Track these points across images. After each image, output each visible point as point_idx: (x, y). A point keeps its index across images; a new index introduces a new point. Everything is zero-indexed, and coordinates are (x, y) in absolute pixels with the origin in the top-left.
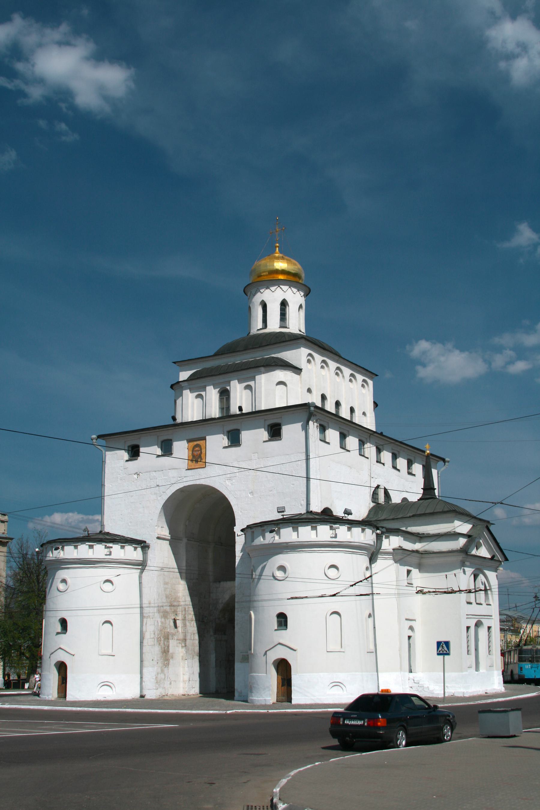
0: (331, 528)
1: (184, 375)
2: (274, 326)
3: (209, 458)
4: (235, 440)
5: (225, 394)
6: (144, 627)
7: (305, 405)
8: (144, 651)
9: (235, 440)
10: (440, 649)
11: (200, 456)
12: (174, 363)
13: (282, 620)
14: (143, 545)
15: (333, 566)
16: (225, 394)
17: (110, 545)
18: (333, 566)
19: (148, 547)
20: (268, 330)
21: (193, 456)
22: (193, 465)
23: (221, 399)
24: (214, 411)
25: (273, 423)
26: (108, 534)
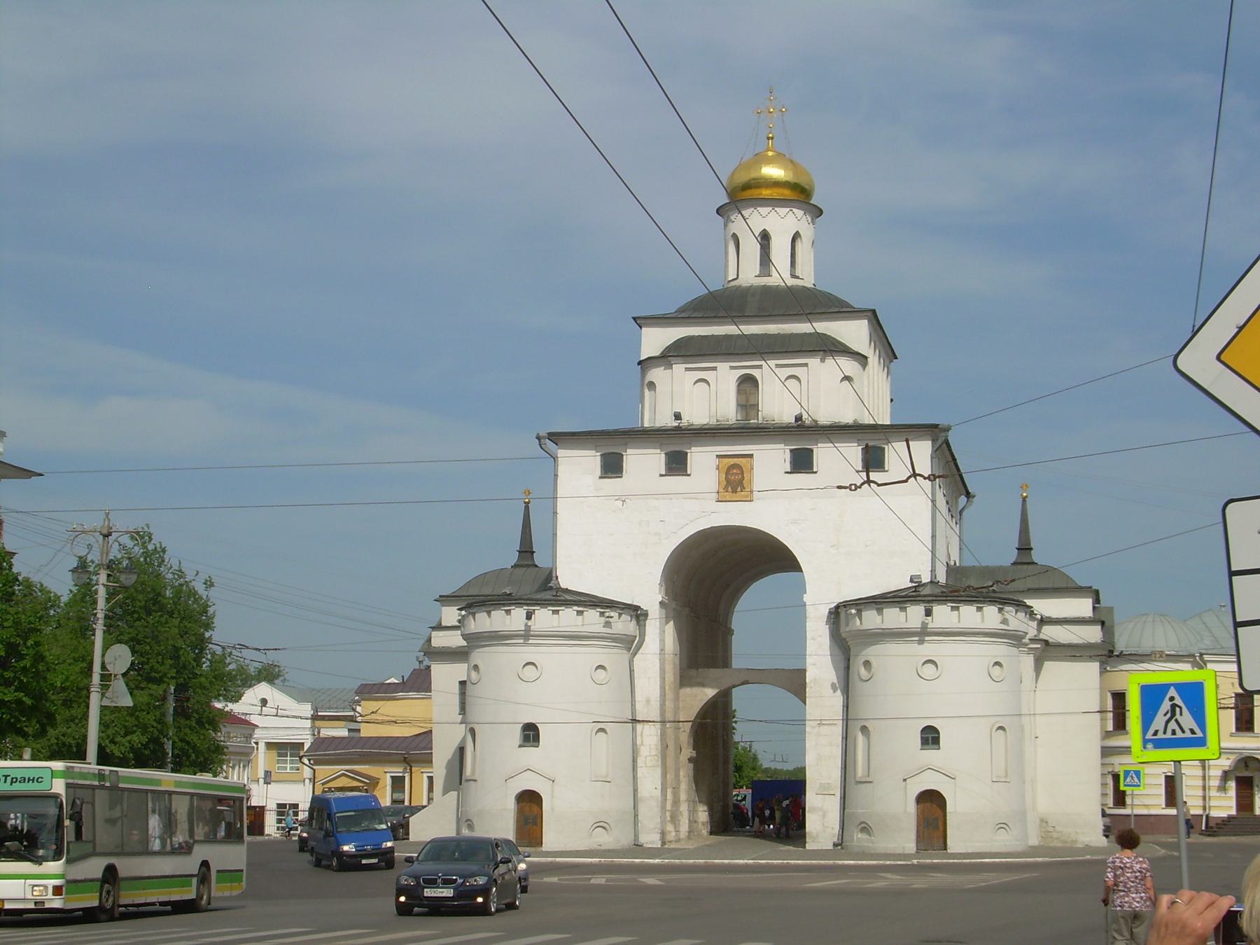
0: (1000, 610)
1: (655, 340)
2: (780, 275)
3: (757, 486)
4: (802, 462)
5: (748, 384)
6: (639, 738)
7: (936, 426)
8: (639, 774)
9: (802, 462)
10: (1129, 779)
11: (741, 483)
12: (634, 319)
13: (930, 737)
14: (638, 614)
15: (997, 663)
16: (748, 384)
17: (609, 613)
18: (997, 663)
19: (646, 615)
20: (774, 280)
21: (728, 482)
22: (728, 496)
23: (740, 391)
24: (727, 410)
25: (872, 444)
26: (567, 591)
